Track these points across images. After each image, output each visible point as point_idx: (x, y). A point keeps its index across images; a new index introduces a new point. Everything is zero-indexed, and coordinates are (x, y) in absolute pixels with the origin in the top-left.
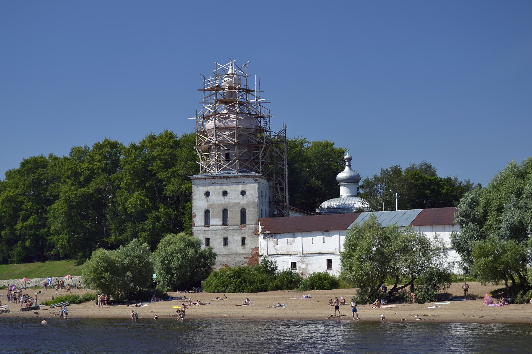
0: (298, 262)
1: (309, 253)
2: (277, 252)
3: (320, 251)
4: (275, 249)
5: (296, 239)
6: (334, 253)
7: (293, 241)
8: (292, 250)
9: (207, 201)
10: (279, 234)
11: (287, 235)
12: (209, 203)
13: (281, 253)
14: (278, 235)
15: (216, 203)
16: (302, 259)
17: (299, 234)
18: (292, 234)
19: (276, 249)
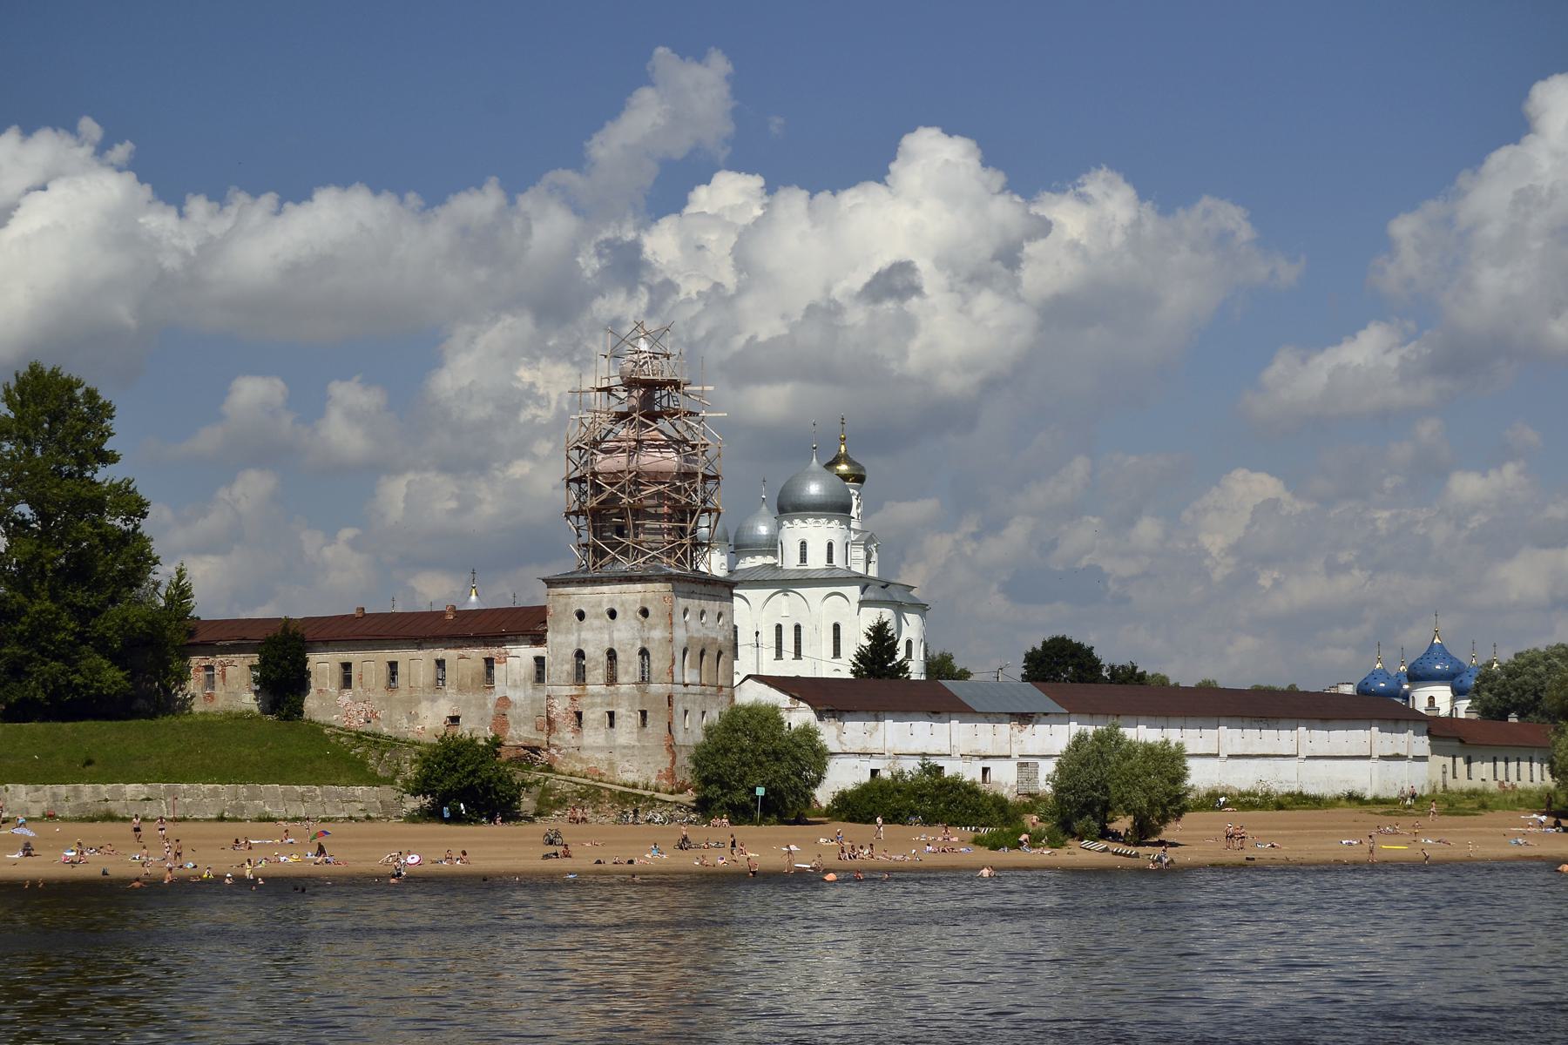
0: (883, 769)
1: (905, 752)
2: (844, 748)
3: (924, 751)
4: (841, 742)
5: (881, 724)
6: (950, 755)
7: (876, 729)
8: (874, 745)
9: (686, 630)
10: (848, 711)
11: (864, 715)
12: (689, 634)
13: (851, 751)
14: (847, 715)
15: (695, 635)
16: (892, 765)
17: (887, 714)
18: (873, 714)
19: (841, 742)
